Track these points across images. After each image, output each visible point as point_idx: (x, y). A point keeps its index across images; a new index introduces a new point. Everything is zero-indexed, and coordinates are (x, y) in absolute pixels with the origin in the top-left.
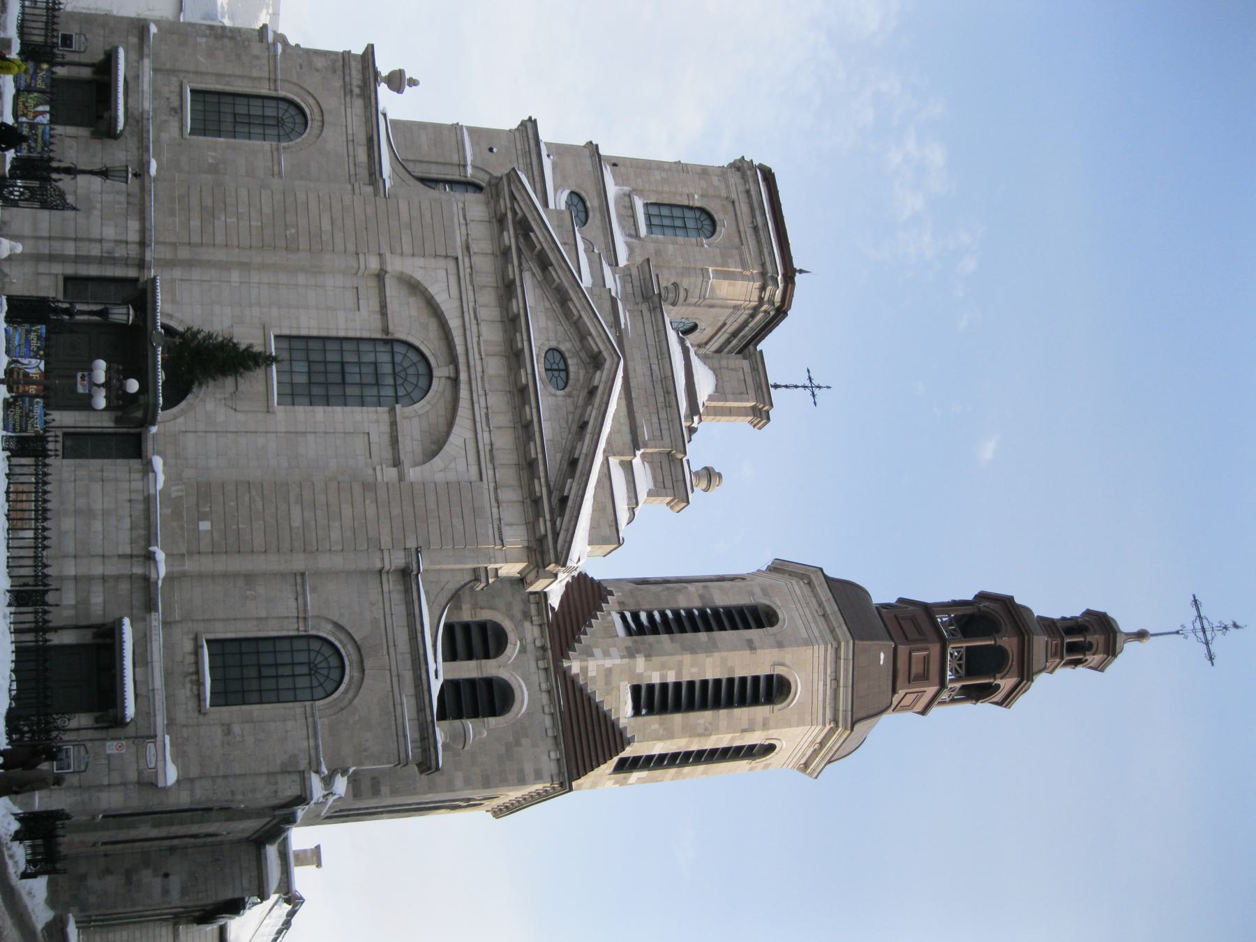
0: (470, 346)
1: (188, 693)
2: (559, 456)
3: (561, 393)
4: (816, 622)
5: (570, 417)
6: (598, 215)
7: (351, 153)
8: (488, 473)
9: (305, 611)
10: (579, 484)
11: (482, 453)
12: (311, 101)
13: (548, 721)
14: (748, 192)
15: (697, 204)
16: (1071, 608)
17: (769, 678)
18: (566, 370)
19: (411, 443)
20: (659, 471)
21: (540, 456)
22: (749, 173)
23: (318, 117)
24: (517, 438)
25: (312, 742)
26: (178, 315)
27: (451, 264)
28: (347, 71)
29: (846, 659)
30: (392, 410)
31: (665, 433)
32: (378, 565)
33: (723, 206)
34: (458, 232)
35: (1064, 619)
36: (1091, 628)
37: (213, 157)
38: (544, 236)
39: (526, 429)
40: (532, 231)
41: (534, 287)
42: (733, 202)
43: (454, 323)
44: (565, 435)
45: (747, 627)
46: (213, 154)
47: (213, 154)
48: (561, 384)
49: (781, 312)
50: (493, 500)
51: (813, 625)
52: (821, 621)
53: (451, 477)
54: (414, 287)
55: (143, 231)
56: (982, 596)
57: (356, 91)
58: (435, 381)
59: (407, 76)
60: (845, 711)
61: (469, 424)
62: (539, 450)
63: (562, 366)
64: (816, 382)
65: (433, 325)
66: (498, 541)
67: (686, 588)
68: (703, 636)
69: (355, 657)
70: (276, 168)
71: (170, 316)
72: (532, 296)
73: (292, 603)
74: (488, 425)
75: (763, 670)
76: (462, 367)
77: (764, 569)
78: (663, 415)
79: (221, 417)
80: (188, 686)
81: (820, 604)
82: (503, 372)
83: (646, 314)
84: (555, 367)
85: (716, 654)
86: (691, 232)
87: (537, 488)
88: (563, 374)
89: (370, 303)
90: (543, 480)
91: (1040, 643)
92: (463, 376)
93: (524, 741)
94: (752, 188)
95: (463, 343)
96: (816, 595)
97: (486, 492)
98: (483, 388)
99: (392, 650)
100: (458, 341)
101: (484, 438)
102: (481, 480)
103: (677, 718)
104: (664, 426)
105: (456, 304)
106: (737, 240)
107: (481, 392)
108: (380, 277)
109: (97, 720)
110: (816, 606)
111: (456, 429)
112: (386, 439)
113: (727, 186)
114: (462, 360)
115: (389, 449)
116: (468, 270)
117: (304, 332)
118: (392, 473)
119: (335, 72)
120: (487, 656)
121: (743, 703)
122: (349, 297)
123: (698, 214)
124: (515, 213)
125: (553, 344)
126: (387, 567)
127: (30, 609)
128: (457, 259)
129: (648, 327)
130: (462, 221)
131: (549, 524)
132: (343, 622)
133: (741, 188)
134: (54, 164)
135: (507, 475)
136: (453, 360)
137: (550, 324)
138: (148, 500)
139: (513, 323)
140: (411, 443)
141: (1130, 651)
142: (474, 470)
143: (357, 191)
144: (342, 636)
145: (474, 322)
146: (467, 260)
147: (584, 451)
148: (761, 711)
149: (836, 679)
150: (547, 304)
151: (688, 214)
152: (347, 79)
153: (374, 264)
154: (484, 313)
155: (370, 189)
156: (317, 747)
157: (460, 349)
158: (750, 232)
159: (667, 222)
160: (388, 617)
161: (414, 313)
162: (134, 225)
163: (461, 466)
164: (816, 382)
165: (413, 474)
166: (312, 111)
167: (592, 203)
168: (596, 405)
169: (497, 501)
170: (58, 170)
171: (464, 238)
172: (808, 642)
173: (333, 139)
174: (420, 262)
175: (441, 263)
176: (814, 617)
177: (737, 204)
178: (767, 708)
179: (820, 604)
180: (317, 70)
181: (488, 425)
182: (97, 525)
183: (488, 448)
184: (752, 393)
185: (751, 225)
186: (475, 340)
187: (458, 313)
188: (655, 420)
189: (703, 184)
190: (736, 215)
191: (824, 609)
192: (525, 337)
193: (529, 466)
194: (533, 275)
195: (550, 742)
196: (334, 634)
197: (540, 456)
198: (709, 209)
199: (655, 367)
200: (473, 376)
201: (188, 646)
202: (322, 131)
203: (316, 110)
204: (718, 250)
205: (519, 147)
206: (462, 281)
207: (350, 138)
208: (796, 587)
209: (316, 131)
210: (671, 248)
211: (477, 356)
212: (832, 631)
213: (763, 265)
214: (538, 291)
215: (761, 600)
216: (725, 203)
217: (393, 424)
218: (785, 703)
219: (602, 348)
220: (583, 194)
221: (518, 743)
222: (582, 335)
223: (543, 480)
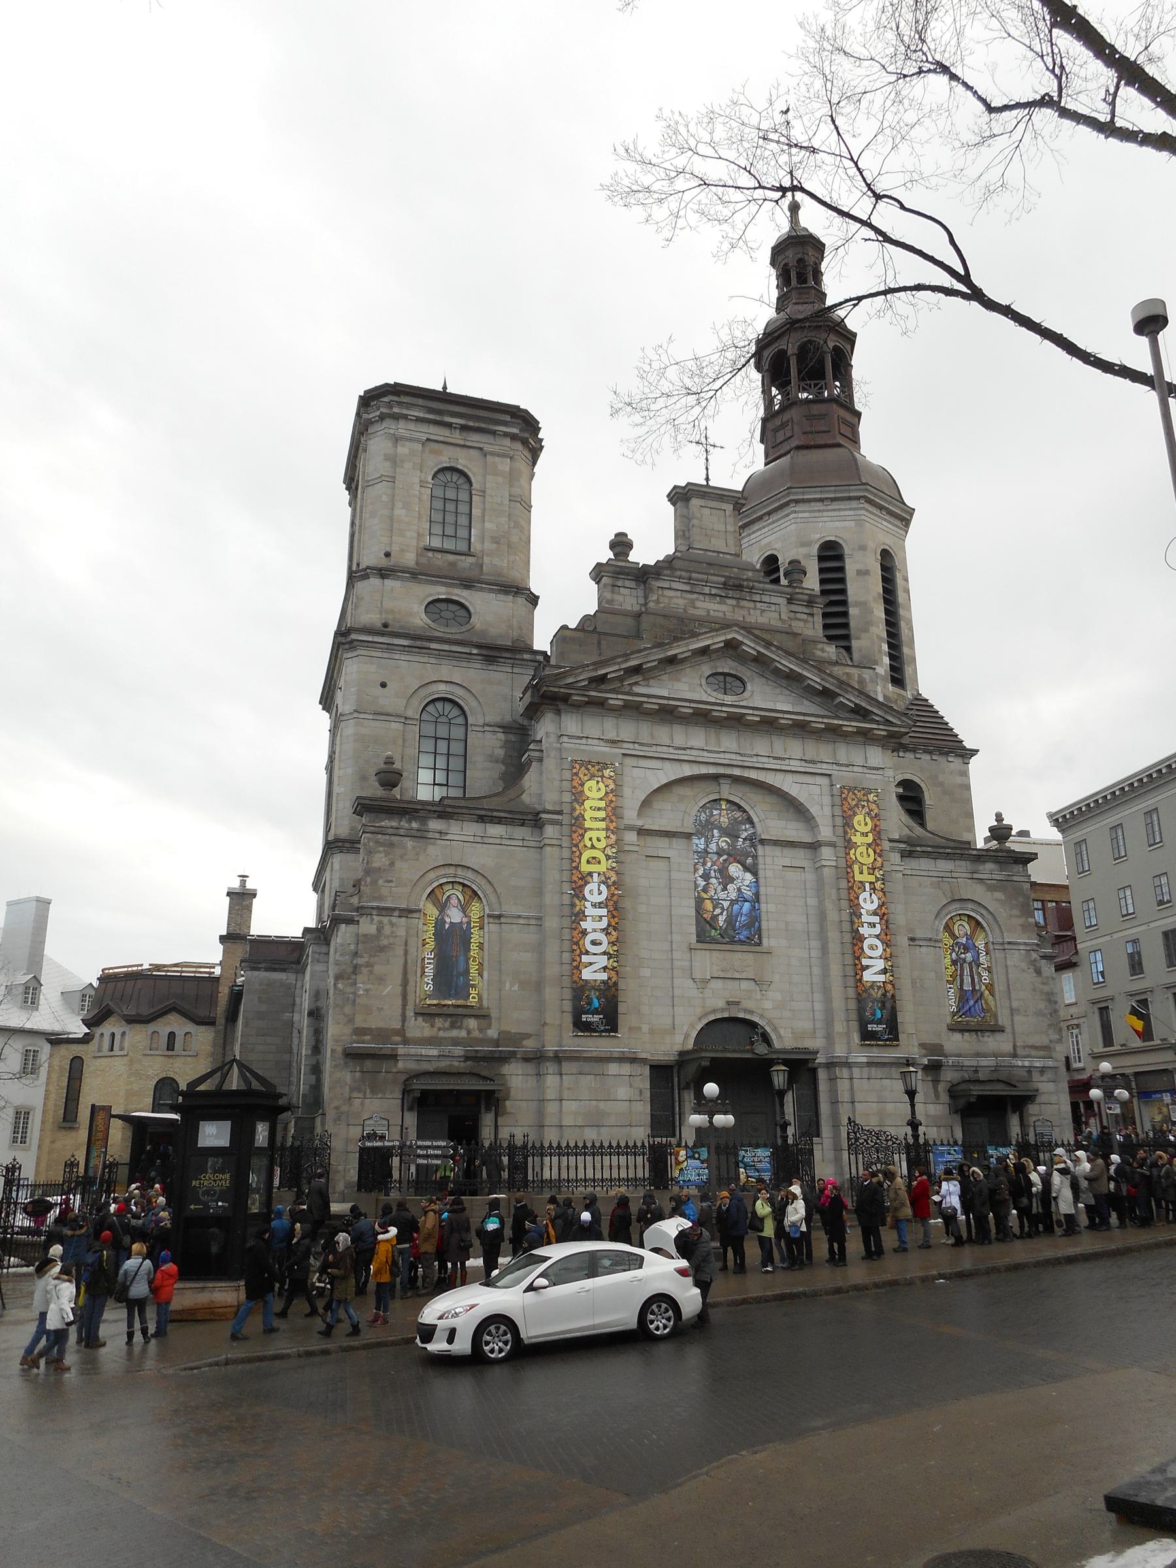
0: (712, 761)
1: (991, 1039)
2: (806, 702)
3: (749, 687)
4: (840, 510)
5: (771, 683)
6: (457, 591)
7: (498, 841)
8: (825, 768)
9: (930, 940)
10: (847, 692)
11: (808, 770)
12: (432, 875)
13: (927, 757)
14: (419, 420)
15: (430, 479)
18: (725, 674)
19: (793, 830)
20: (798, 615)
21: (826, 721)
22: (396, 410)
23: (451, 871)
24: (794, 736)
25: (1022, 947)
26: (685, 1028)
27: (628, 761)
28: (390, 831)
29: (876, 495)
30: (763, 842)
31: (774, 600)
32: (900, 875)
33: (432, 452)
34: (595, 748)
37: (512, 985)
38: (615, 664)
39: (769, 725)
40: (607, 674)
41: (648, 686)
42: (428, 440)
43: (688, 770)
44: (788, 692)
45: (842, 569)
46: (508, 985)
47: (508, 985)
48: (738, 683)
50: (847, 769)
51: (842, 513)
52: (835, 505)
53: (827, 800)
54: (646, 803)
55: (622, 1059)
57: (414, 825)
59: (382, 766)
61: (780, 776)
62: (820, 720)
63: (721, 678)
64: (711, 441)
66: (880, 772)
68: (853, 611)
69: (957, 905)
70: (522, 921)
71: (687, 1036)
72: (662, 689)
73: (923, 949)
74: (784, 759)
76: (729, 771)
78: (757, 598)
79: (778, 996)
80: (986, 1039)
81: (821, 500)
82: (734, 735)
83: (661, 584)
84: (722, 685)
85: (873, 604)
87: (850, 729)
88: (729, 679)
89: (661, 846)
90: (845, 723)
92: (737, 772)
93: (941, 778)
94: (416, 414)
95: (705, 766)
96: (809, 501)
97: (840, 773)
98: (751, 756)
99: (954, 875)
100: (704, 770)
101: (795, 765)
102: (830, 775)
103: (905, 650)
104: (766, 599)
105: (667, 764)
106: (472, 451)
107: (755, 759)
108: (641, 832)
109: (1014, 1112)
110: (820, 504)
112: (788, 852)
113: (411, 440)
114: (722, 770)
115: (797, 850)
116: (636, 745)
117: (693, 913)
118: (826, 852)
119: (392, 845)
122: (654, 864)
125: (704, 681)
126: (901, 868)
127: (647, 1175)
128: (623, 754)
129: (675, 585)
130: (584, 741)
131: (881, 727)
132: (935, 910)
133: (412, 426)
134: (911, 1141)
135: (821, 751)
136: (716, 778)
137: (684, 680)
138: (869, 1064)
139: (667, 714)
142: (819, 780)
143: (554, 842)
144: (944, 912)
145: (688, 752)
146: (625, 745)
147: (818, 680)
149: (881, 508)
150: (665, 677)
152: (402, 832)
153: (631, 837)
154: (679, 740)
155: (549, 831)
156: (1025, 944)
157: (712, 770)
158: (465, 434)
159: (450, 518)
160: (931, 874)
161: (668, 806)
162: (613, 1068)
163: (817, 790)
164: (711, 441)
166: (444, 876)
167: (441, 592)
168: (778, 659)
169: (848, 766)
170: (916, 1136)
171: (602, 743)
172: (859, 523)
173: (481, 857)
174: (627, 792)
175: (627, 770)
176: (834, 510)
177: (432, 437)
179: (821, 500)
180: (392, 864)
181: (784, 759)
182: (890, 1107)
183: (803, 764)
184: (724, 506)
185: (458, 431)
186: (705, 754)
187: (677, 765)
188: (759, 605)
189: (408, 465)
190: (443, 442)
191: (827, 498)
192: (719, 708)
193: (833, 733)
194: (636, 683)
195: (941, 759)
196: (942, 919)
197: (826, 721)
198: (436, 469)
199: (714, 591)
200: (740, 763)
201: (957, 1036)
202: (468, 868)
203: (442, 871)
204: (489, 478)
205: (379, 654)
207: (479, 839)
208: (801, 515)
209: (470, 874)
210: (488, 525)
211: (722, 756)
212: (850, 498)
213: (506, 435)
214: (652, 682)
215: (814, 550)
216: (427, 449)
217: (776, 843)
219: (723, 638)
220: (431, 599)
221: (941, 784)
222: (704, 651)
223: (845, 723)
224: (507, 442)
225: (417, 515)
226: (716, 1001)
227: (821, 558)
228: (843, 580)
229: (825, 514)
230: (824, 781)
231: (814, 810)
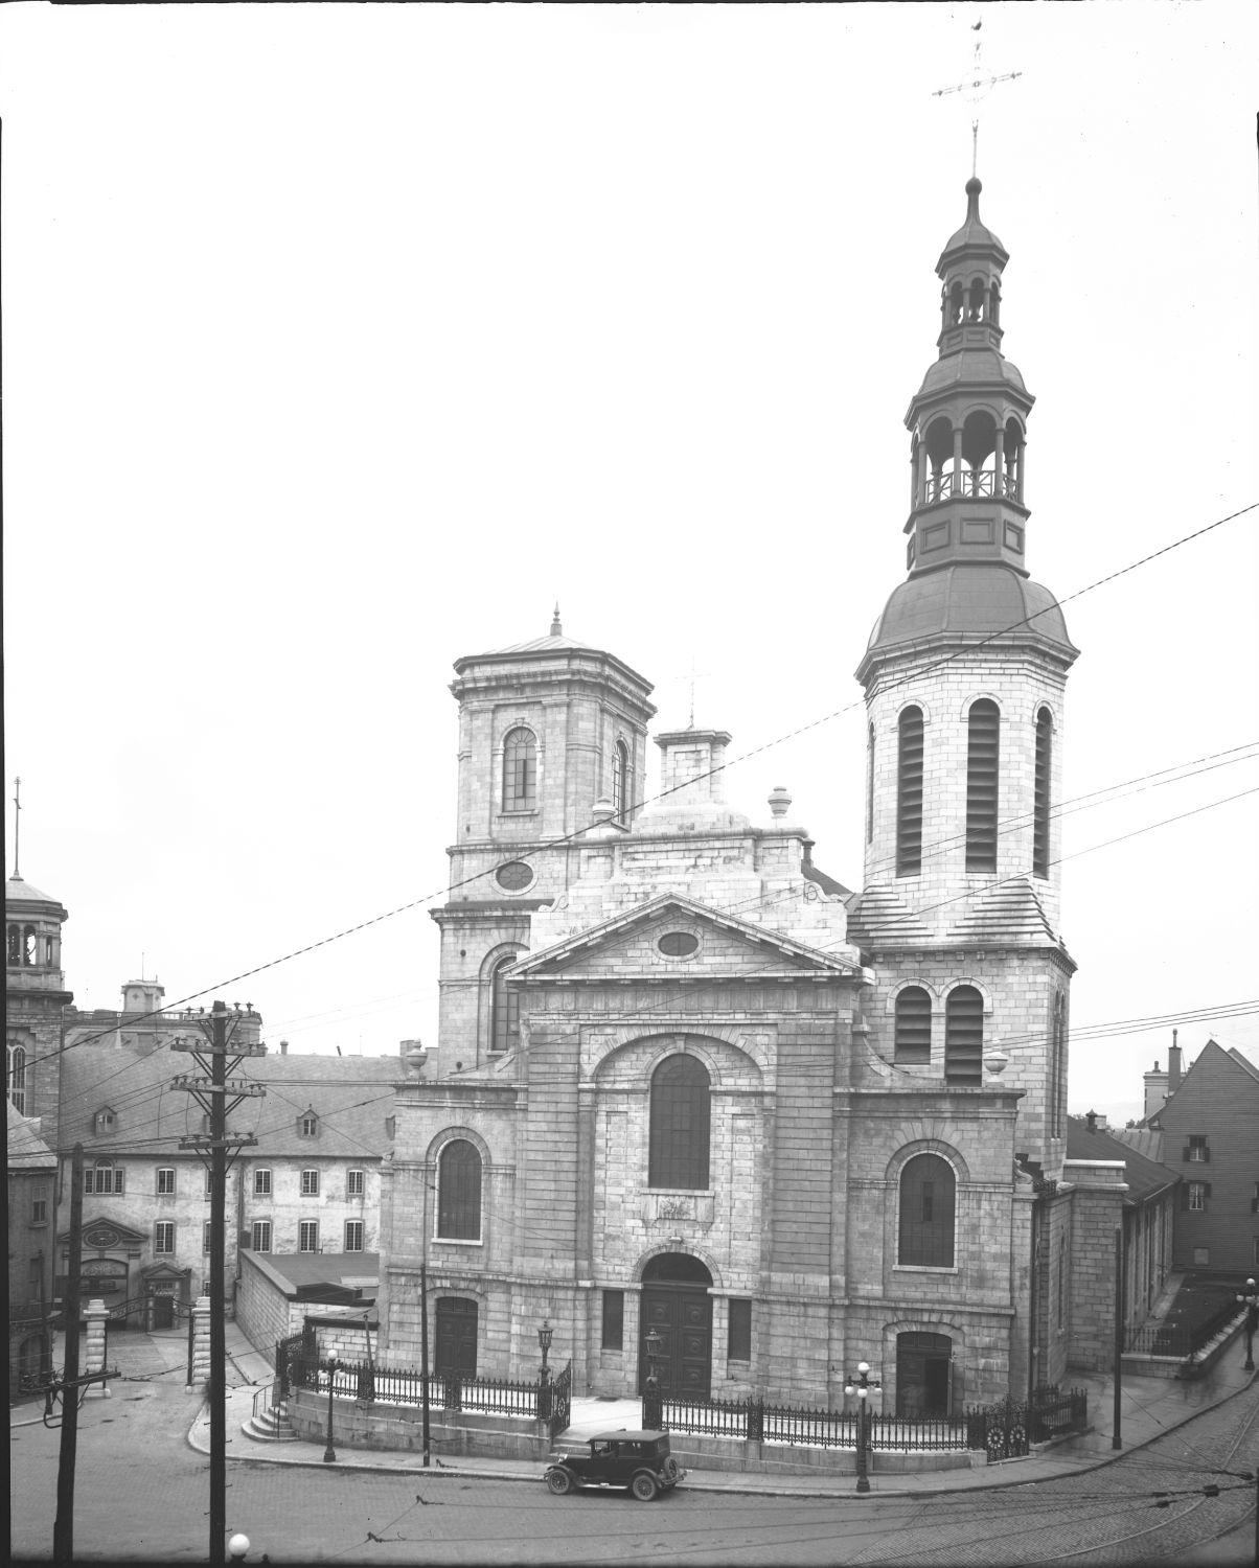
16: (934, 289)
17: (972, 719)
27: (587, 1032)
35: (943, 308)
42: (497, 706)
45: (920, 738)
56: (910, 423)
67: (879, 796)
86: (530, 756)
92: (685, 1030)
107: (699, 1017)
113: (481, 712)
114: (675, 1030)
121: (994, 748)
124: (536, 972)
128: (581, 1025)
140: (744, 1083)
148: (1004, 729)
151: (512, 756)
157: (662, 1030)
174: (584, 1058)
177: (502, 702)
178: (1003, 727)
196: (901, 1161)
206: (601, 1022)
215: (894, 721)
218: (1000, 706)
225: (488, 786)
228: (920, 752)
230: (772, 1032)
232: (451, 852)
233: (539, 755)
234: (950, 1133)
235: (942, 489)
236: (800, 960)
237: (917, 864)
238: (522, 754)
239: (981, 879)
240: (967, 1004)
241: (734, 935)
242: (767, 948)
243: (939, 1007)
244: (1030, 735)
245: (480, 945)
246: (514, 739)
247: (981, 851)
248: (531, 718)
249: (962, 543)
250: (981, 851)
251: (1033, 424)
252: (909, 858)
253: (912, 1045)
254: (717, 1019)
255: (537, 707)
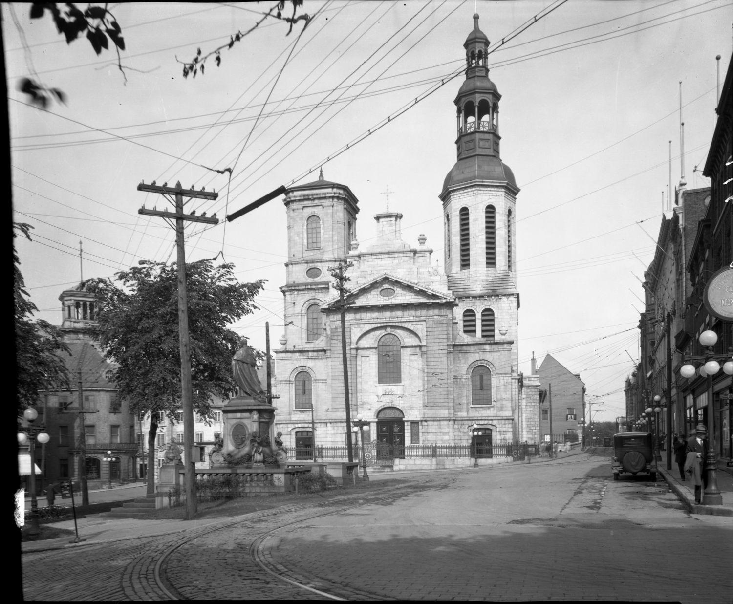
8: (422, 318)
17: (487, 212)
19: (413, 341)
36: (473, 49)
42: (304, 207)
49: (345, 188)
56: (457, 102)
58: (392, 333)
60: (500, 183)
61: (407, 323)
65: (372, 333)
75: (484, 215)
77: (442, 202)
83: (365, 258)
86: (318, 226)
91: (479, 83)
92: (391, 324)
100: (379, 325)
111: (409, 327)
114: (385, 324)
120: (475, 315)
123: (309, 222)
133: (297, 203)
136: (384, 327)
141: (481, 28)
151: (310, 226)
157: (382, 325)
159: (314, 235)
165: (424, 343)
173: (310, 363)
224: (331, 200)
226: (385, 402)
227: (462, 215)
228: (468, 224)
229: (463, 195)
230: (424, 323)
231: (420, 335)
232: (287, 265)
233: (322, 226)
234: (488, 357)
235: (470, 127)
236: (434, 296)
237: (468, 265)
238: (314, 225)
239: (491, 271)
240: (488, 314)
241: (409, 288)
242: (422, 293)
243: (479, 316)
244: (505, 218)
245: (303, 298)
246: (310, 219)
247: (491, 260)
248: (317, 211)
249: (479, 148)
250: (491, 260)
251: (501, 103)
252: (465, 263)
253: (469, 329)
254: (404, 319)
255: (321, 207)
